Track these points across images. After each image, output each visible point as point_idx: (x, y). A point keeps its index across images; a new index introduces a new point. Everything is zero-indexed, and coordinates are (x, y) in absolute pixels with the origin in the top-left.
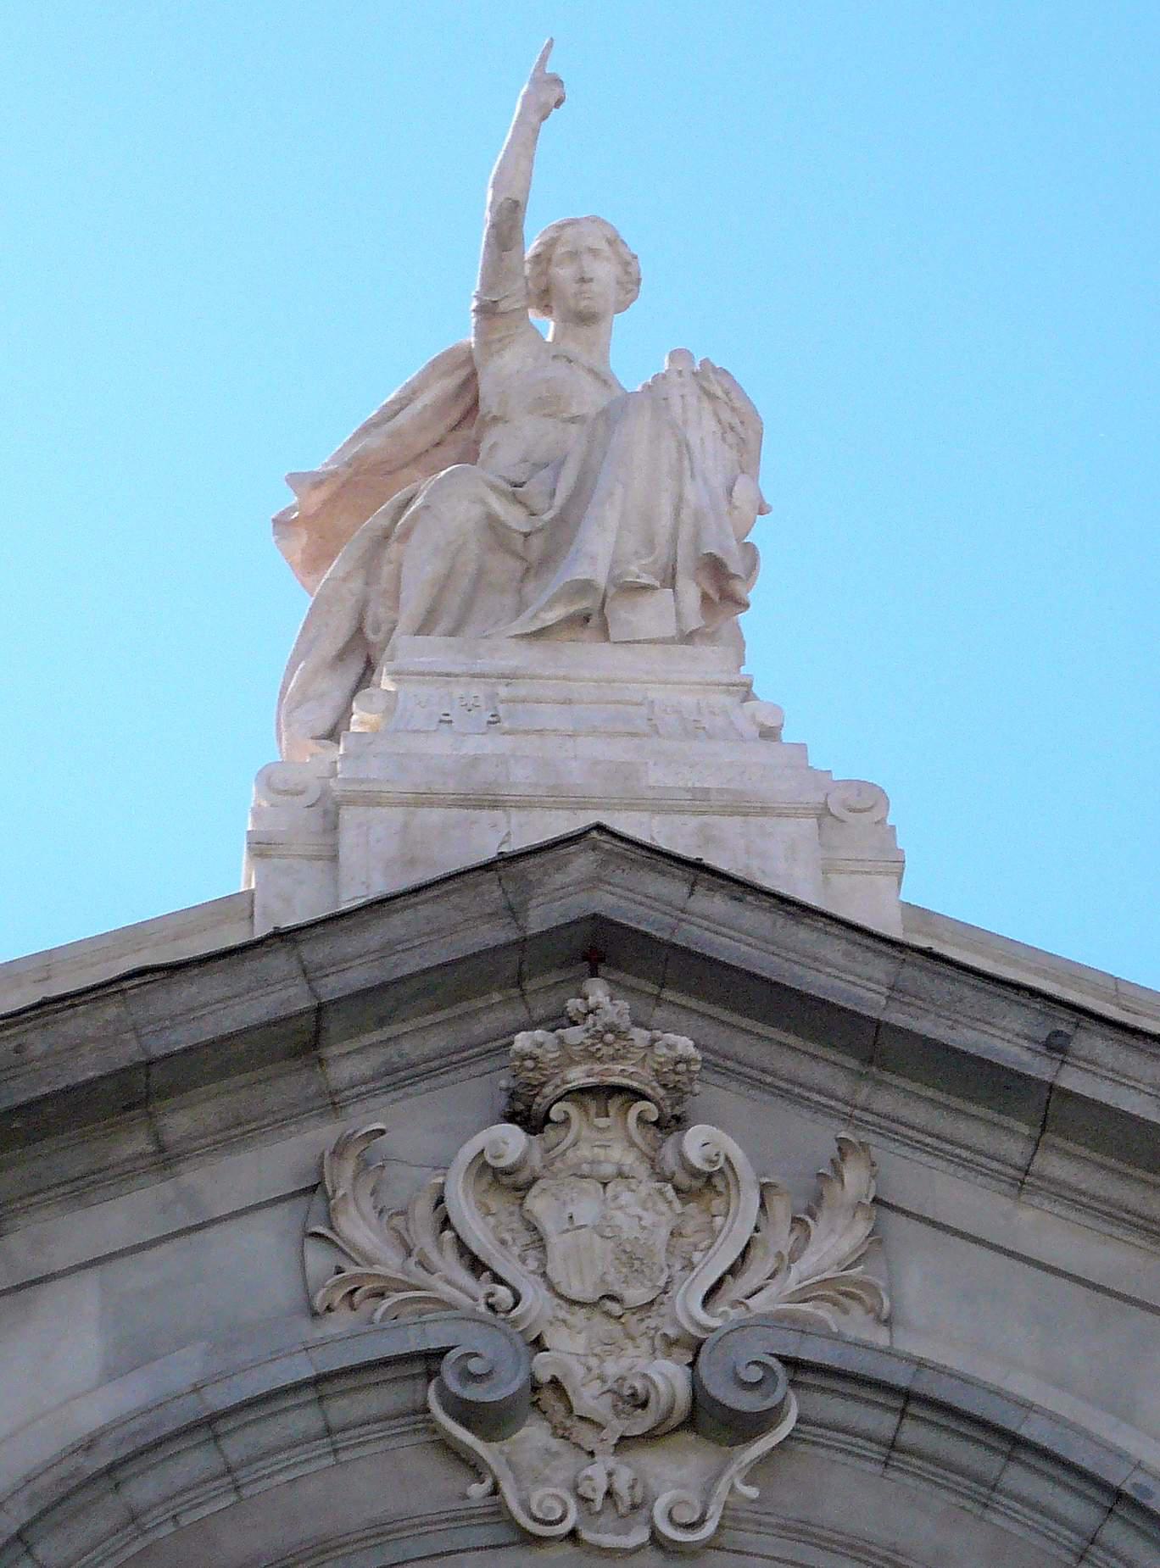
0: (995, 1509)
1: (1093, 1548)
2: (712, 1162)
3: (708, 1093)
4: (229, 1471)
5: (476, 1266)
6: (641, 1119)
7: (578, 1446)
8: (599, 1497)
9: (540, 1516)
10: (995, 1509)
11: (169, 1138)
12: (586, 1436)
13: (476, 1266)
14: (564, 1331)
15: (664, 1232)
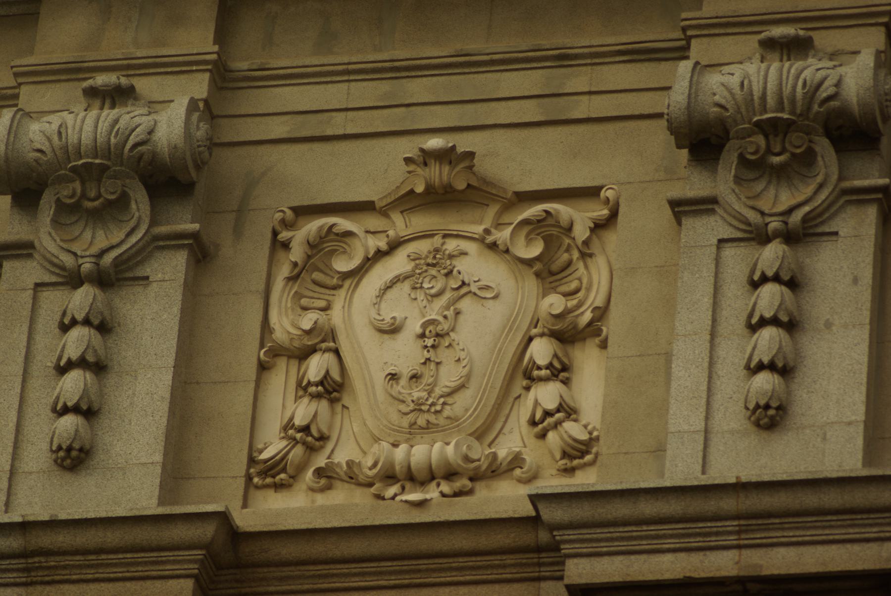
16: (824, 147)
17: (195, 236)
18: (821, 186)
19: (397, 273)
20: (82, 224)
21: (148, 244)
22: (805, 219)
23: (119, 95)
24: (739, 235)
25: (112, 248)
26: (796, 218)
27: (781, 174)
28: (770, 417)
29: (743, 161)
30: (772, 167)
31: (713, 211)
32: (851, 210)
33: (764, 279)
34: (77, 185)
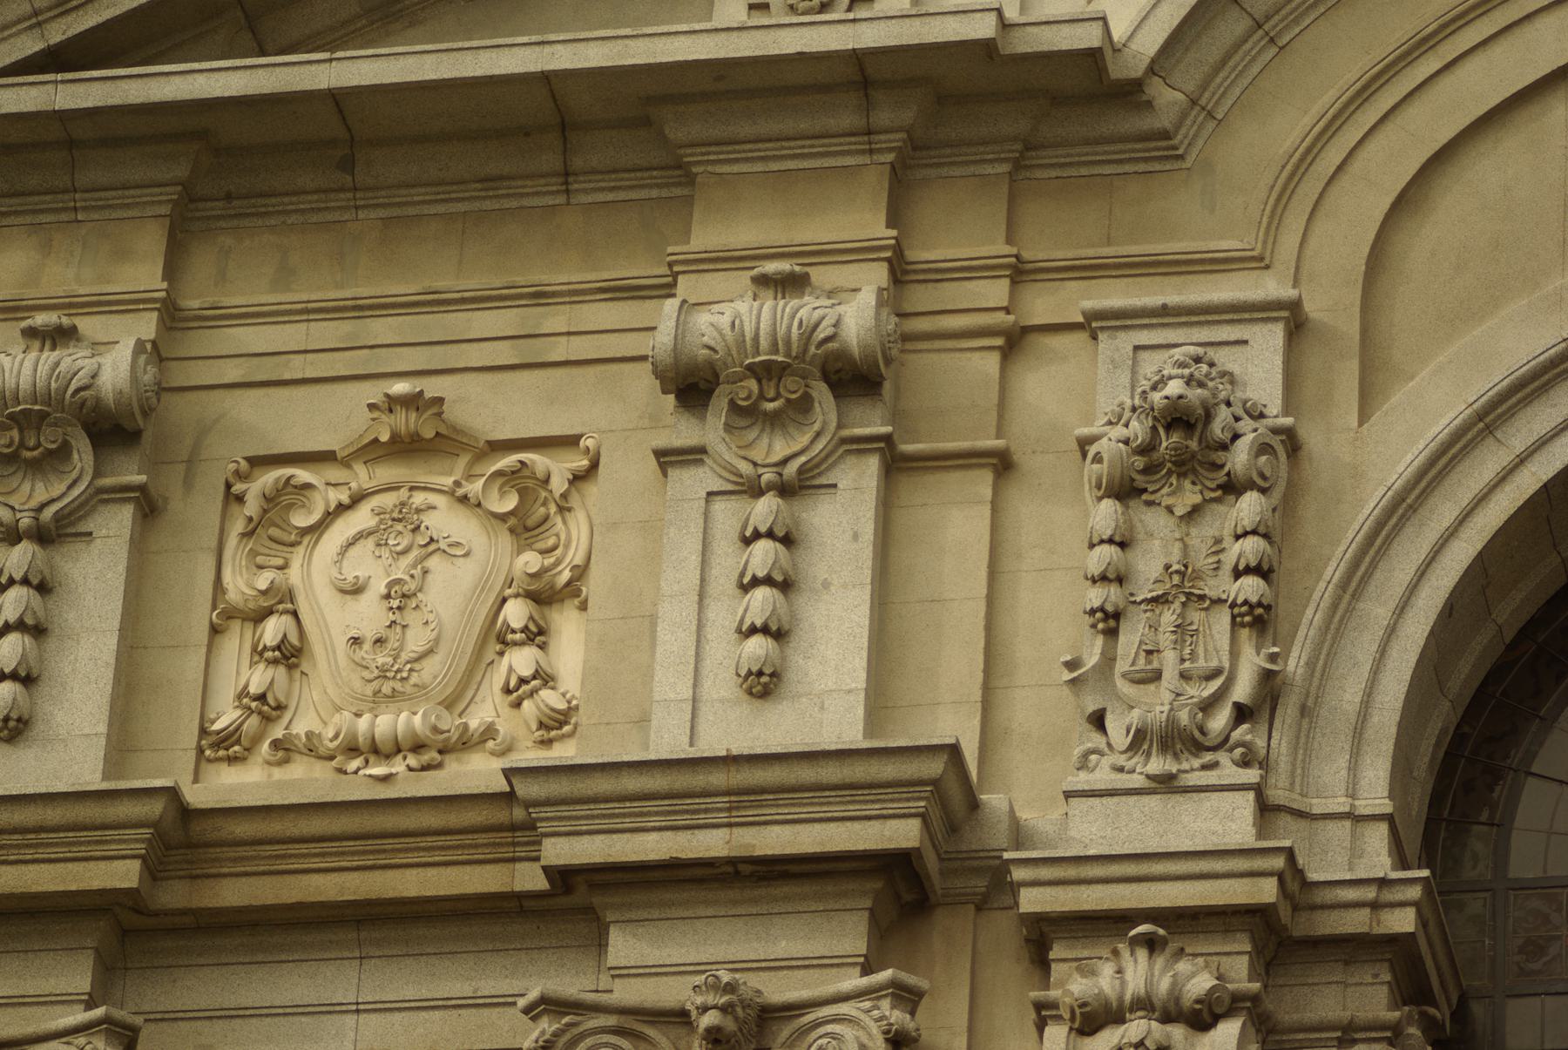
16: (822, 393)
17: (142, 488)
18: (818, 435)
19: (359, 528)
20: (20, 475)
21: (91, 497)
22: (801, 471)
23: (61, 336)
24: (730, 487)
25: (53, 501)
26: (791, 469)
27: (774, 421)
28: (763, 685)
29: (734, 407)
30: (765, 413)
31: (701, 461)
32: (851, 460)
33: (757, 535)
34: (15, 434)
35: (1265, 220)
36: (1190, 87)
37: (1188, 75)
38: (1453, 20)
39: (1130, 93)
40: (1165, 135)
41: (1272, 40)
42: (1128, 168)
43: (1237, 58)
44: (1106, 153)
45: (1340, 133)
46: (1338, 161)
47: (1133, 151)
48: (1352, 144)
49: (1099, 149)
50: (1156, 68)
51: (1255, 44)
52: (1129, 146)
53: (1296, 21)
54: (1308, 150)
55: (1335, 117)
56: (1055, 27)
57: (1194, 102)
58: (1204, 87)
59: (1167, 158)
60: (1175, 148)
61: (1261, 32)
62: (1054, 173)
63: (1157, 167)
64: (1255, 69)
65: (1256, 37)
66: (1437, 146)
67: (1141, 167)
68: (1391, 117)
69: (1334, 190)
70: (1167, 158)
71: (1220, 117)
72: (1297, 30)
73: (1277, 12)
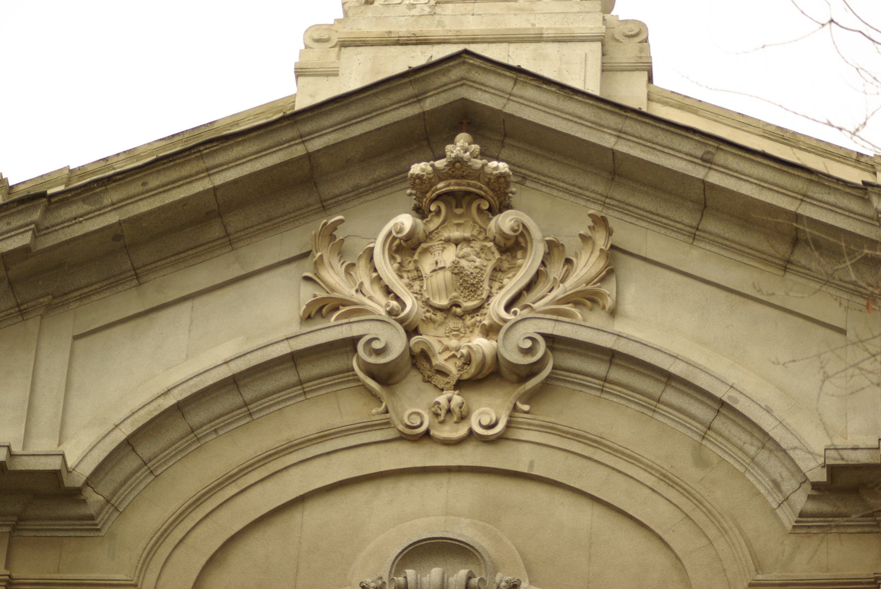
0: (658, 412)
1: (709, 432)
2: (515, 231)
3: (518, 194)
4: (246, 405)
5: (388, 291)
6: (479, 209)
7: (436, 386)
8: (443, 413)
9: (409, 424)
10: (658, 412)
11: (231, 230)
12: (439, 380)
13: (388, 291)
14: (431, 325)
15: (489, 269)
35: (140, 566)
36: (107, 494)
37: (106, 487)
38: (247, 467)
39: (75, 495)
40: (92, 518)
41: (152, 472)
42: (71, 534)
43: (132, 480)
44: (60, 525)
45: (183, 523)
46: (180, 537)
47: (75, 525)
48: (188, 529)
49: (57, 522)
50: (89, 482)
51: (143, 473)
52: (73, 522)
53: (165, 463)
54: (165, 530)
55: (181, 514)
56: (37, 458)
57: (108, 502)
58: (114, 494)
59: (92, 530)
60: (96, 525)
61: (146, 467)
62: (32, 534)
63: (86, 534)
64: (142, 487)
65: (143, 470)
66: (233, 533)
67: (79, 534)
68: (210, 516)
69: (178, 552)
70: (92, 530)
71: (121, 510)
72: (165, 468)
73: (155, 457)
